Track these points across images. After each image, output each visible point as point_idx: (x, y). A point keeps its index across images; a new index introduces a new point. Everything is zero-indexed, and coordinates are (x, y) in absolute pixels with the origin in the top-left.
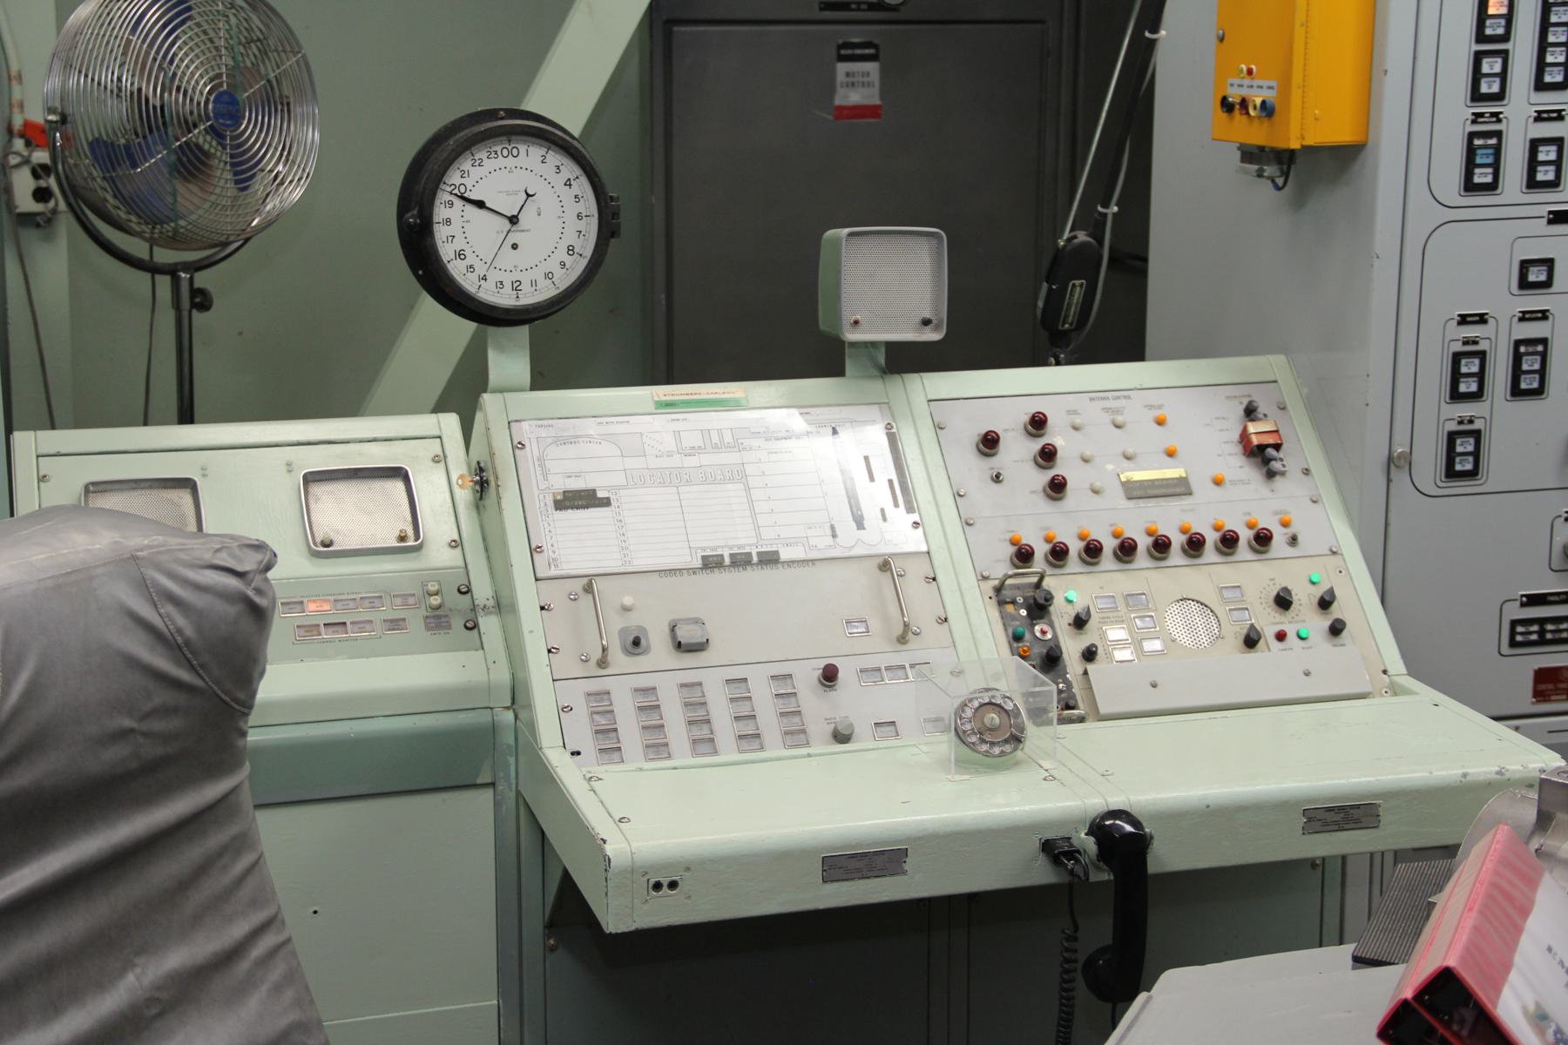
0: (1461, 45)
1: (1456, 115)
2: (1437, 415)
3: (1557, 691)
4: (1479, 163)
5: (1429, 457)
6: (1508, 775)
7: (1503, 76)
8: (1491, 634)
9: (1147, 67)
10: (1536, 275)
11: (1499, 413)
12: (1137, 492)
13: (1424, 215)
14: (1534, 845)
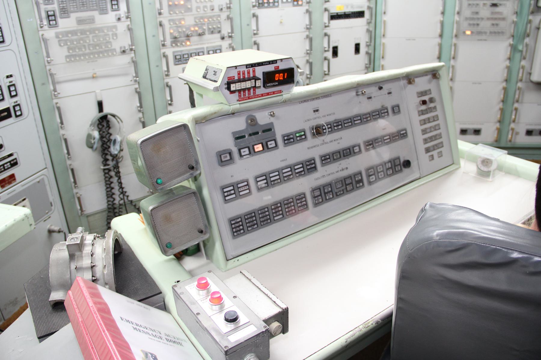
3: (6, 184)
6: (17, 220)
14: (73, 266)
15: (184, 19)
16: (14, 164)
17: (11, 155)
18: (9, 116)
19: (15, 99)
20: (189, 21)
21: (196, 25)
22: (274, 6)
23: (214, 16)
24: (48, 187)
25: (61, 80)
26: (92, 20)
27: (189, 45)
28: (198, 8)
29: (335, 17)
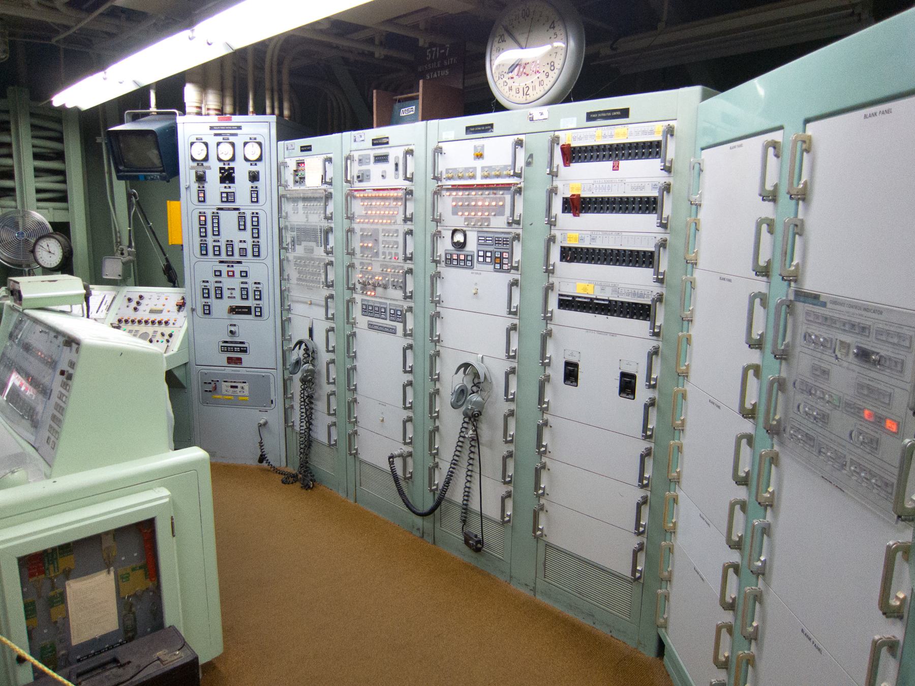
0: (196, 226)
1: (197, 240)
2: (200, 301)
4: (204, 248)
5: (200, 310)
7: (206, 232)
8: (216, 348)
9: (110, 225)
10: (218, 273)
11: (213, 301)
12: (152, 311)
13: (194, 260)
15: (370, 264)
16: (244, 351)
17: (243, 343)
18: (249, 313)
19: (258, 302)
20: (377, 268)
21: (380, 274)
22: (465, 267)
23: (398, 266)
24: (272, 386)
25: (294, 298)
26: (312, 251)
27: (374, 296)
28: (384, 253)
29: (567, 303)
